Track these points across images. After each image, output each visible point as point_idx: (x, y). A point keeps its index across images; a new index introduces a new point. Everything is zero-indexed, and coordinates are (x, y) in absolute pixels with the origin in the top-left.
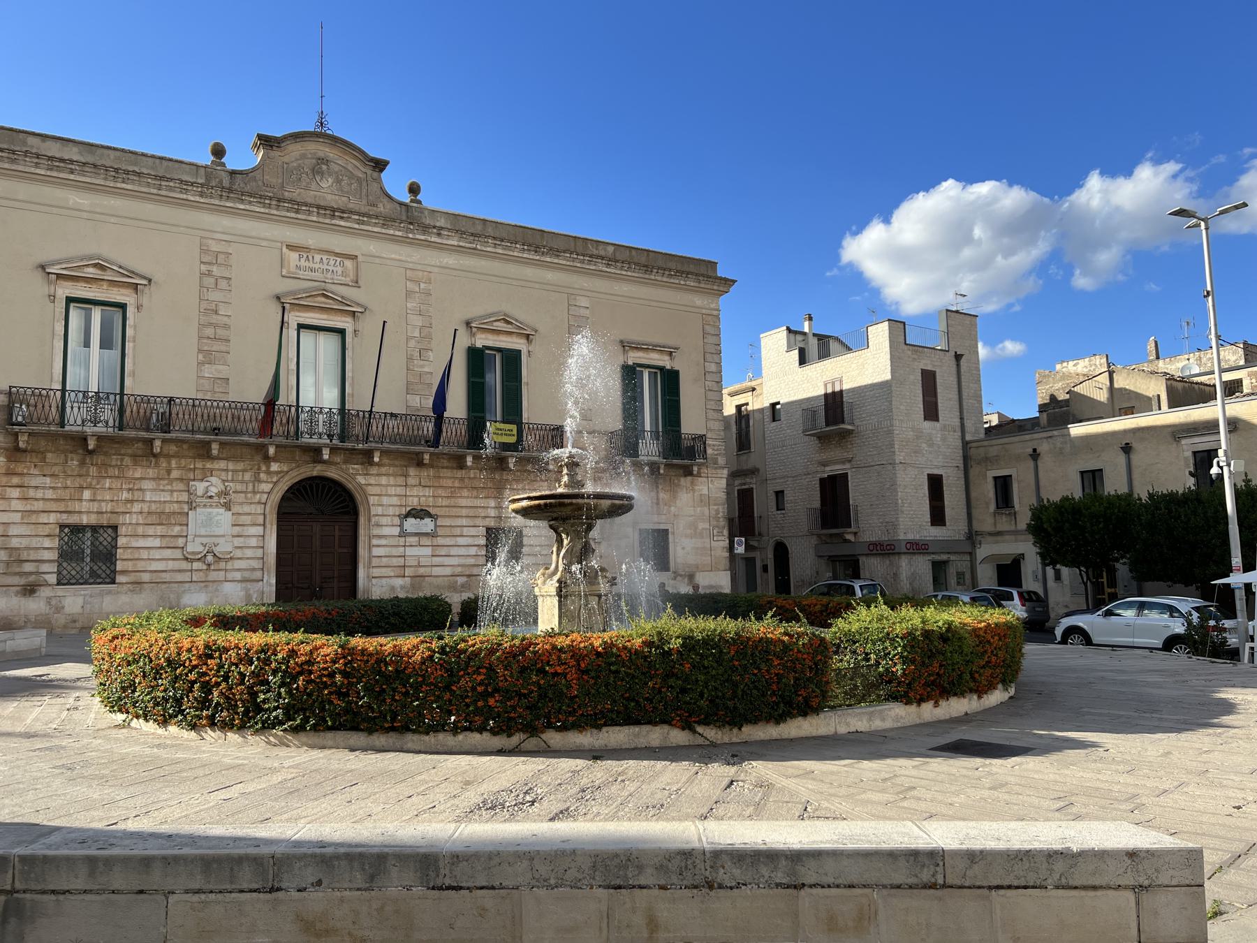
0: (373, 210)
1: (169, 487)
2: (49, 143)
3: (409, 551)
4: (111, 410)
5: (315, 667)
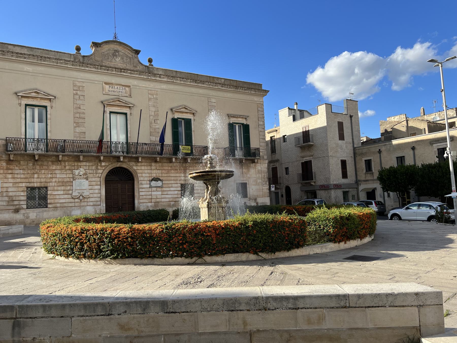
0: (135, 69)
1: (65, 172)
2: (16, 48)
3: (153, 193)
4: (43, 145)
5: (121, 236)
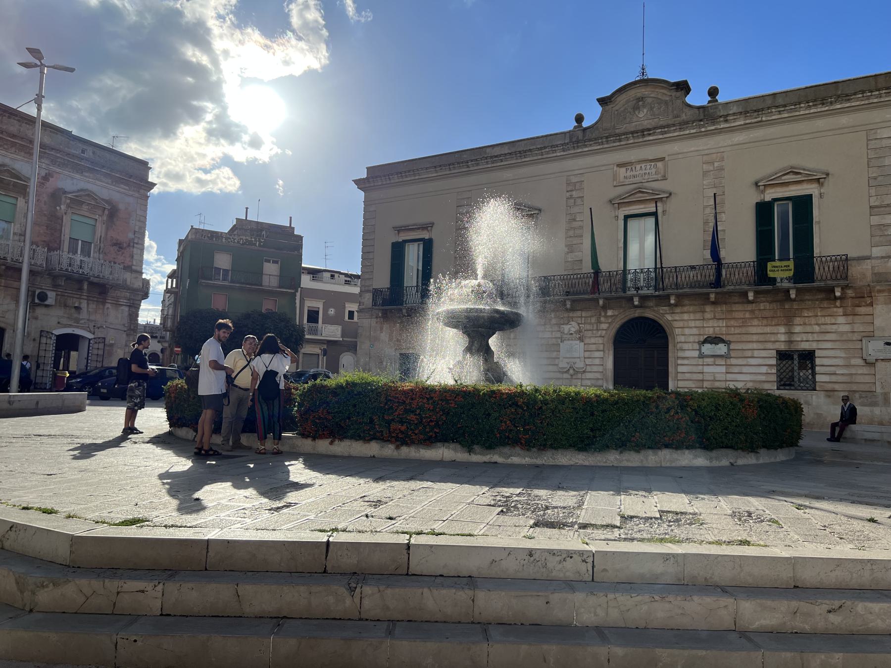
2: (496, 149)
3: (706, 369)
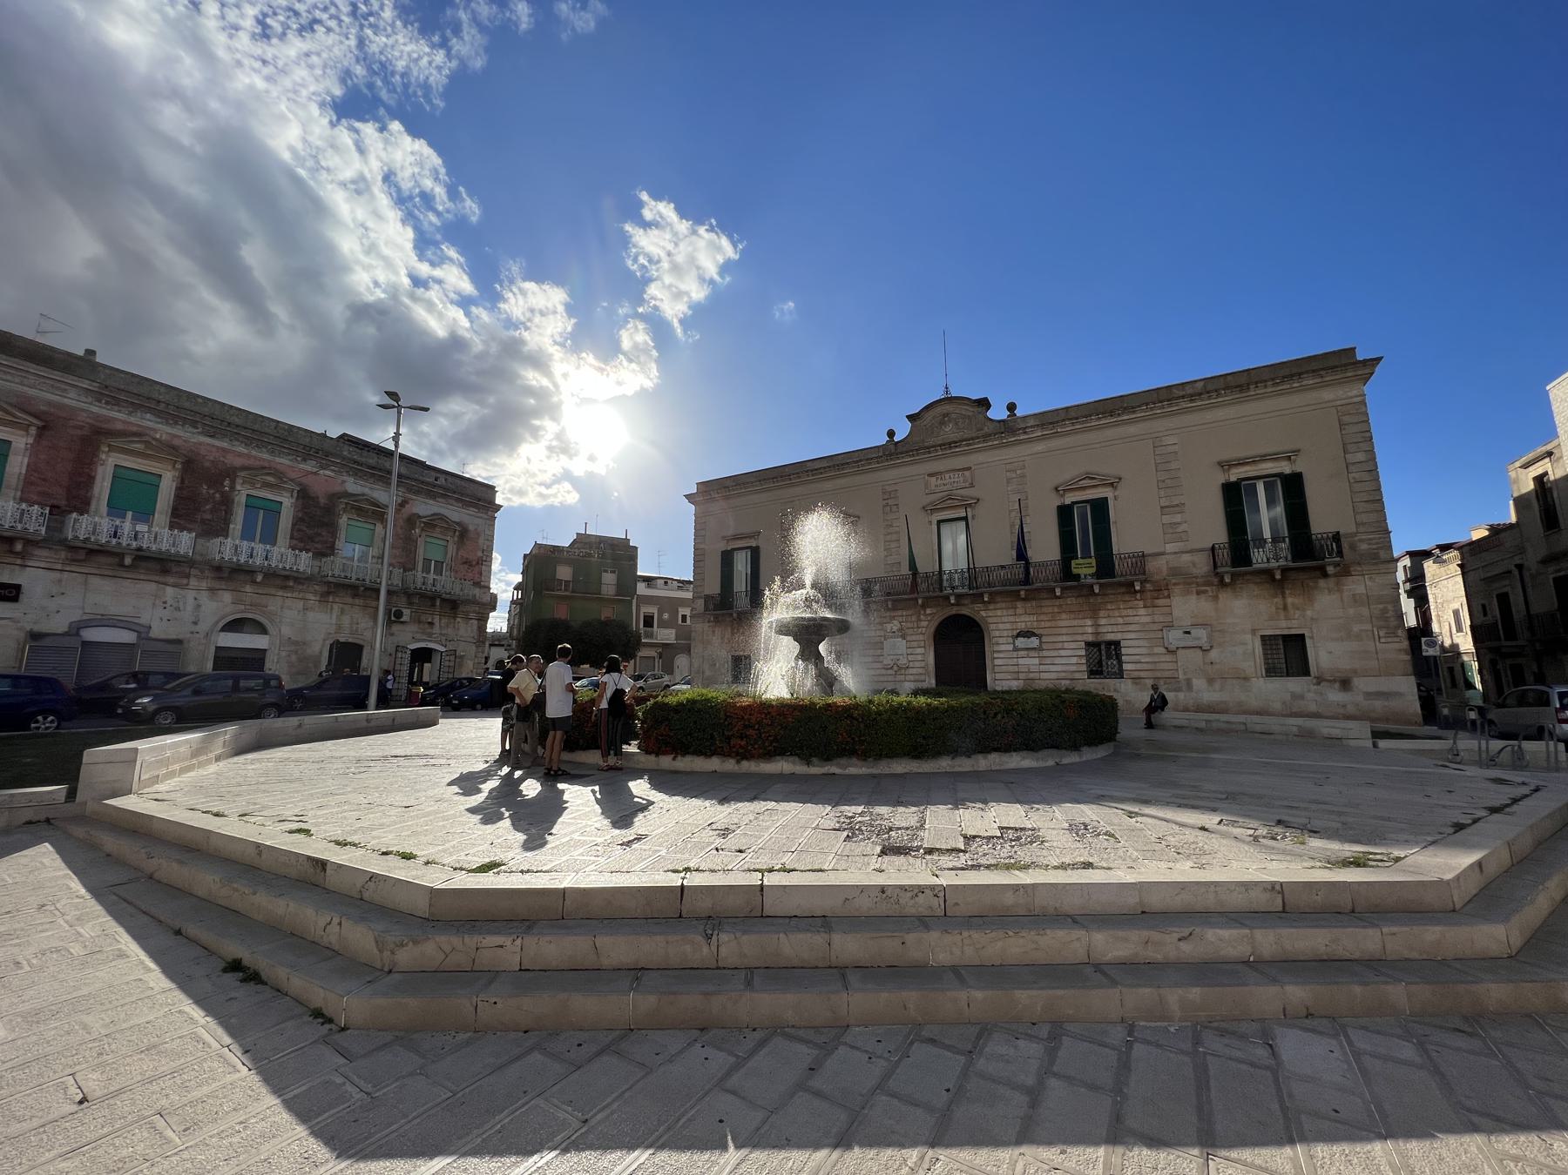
0: (980, 433)
3: (1021, 661)
